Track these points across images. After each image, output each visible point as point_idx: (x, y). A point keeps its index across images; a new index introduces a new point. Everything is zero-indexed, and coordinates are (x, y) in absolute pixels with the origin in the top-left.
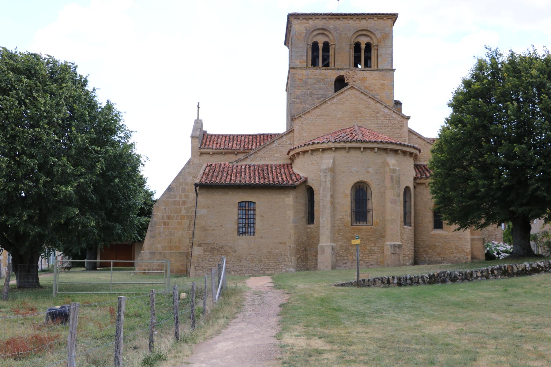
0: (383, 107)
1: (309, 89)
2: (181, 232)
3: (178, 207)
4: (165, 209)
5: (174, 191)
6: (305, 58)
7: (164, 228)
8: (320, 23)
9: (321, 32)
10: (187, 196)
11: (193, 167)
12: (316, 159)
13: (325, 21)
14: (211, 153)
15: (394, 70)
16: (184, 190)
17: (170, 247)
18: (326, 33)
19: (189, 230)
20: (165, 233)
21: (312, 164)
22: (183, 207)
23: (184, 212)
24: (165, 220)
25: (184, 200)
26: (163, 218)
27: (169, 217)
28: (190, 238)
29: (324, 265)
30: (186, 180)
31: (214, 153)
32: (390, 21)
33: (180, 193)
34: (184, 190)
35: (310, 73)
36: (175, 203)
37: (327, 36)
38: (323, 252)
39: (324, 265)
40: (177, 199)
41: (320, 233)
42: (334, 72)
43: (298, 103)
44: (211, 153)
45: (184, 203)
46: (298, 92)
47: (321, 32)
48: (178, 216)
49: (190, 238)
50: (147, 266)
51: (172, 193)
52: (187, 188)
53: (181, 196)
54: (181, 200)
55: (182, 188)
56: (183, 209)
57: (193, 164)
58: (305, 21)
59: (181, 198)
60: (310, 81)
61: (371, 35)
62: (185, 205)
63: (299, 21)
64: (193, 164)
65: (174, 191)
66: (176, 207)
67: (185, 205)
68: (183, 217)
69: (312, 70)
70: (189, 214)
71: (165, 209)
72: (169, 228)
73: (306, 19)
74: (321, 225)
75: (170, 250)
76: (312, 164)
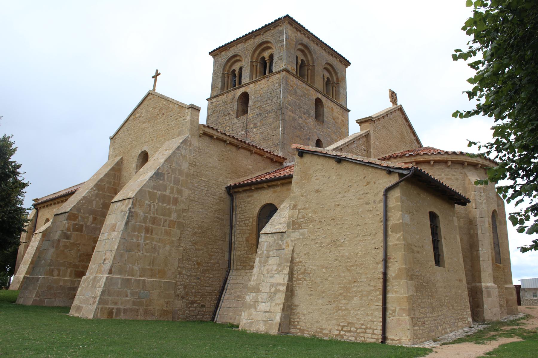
0: (415, 138)
1: (298, 100)
2: (168, 247)
3: (168, 207)
4: (150, 205)
5: (164, 180)
6: (295, 66)
7: (146, 238)
8: (306, 41)
9: (302, 48)
10: (180, 192)
11: (191, 150)
12: (455, 173)
13: (308, 40)
14: (215, 137)
15: (349, 111)
16: (176, 182)
17: (152, 270)
18: (306, 51)
19: (180, 246)
20: (147, 247)
21: (447, 178)
22: (173, 207)
23: (174, 216)
24: (147, 225)
25: (176, 196)
26: (145, 220)
27: (154, 221)
28: (179, 259)
29: (492, 312)
30: (180, 166)
31: (218, 139)
32: (344, 66)
33: (172, 184)
34: (176, 182)
35: (299, 84)
36: (164, 199)
37: (305, 55)
38: (489, 295)
39: (492, 312)
40: (167, 193)
41: (482, 269)
42: (315, 92)
43: (290, 110)
44: (215, 137)
45: (176, 201)
46: (290, 98)
47: (302, 48)
48: (165, 221)
49: (179, 259)
50: (116, 303)
51: (161, 182)
52: (181, 178)
53: (172, 189)
54: (172, 196)
55: (175, 178)
56: (173, 211)
57: (190, 146)
58: (295, 30)
59: (172, 193)
60: (299, 92)
61: (333, 73)
62: (176, 205)
63: (291, 28)
64: (190, 146)
65: (164, 180)
66: (165, 205)
67: (176, 205)
68: (172, 224)
69: (300, 82)
70: (181, 220)
71: (150, 205)
72: (152, 239)
73: (297, 29)
74: (481, 259)
75: (151, 276)
76: (447, 178)
